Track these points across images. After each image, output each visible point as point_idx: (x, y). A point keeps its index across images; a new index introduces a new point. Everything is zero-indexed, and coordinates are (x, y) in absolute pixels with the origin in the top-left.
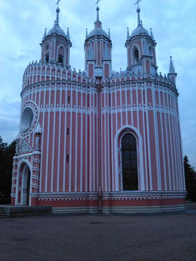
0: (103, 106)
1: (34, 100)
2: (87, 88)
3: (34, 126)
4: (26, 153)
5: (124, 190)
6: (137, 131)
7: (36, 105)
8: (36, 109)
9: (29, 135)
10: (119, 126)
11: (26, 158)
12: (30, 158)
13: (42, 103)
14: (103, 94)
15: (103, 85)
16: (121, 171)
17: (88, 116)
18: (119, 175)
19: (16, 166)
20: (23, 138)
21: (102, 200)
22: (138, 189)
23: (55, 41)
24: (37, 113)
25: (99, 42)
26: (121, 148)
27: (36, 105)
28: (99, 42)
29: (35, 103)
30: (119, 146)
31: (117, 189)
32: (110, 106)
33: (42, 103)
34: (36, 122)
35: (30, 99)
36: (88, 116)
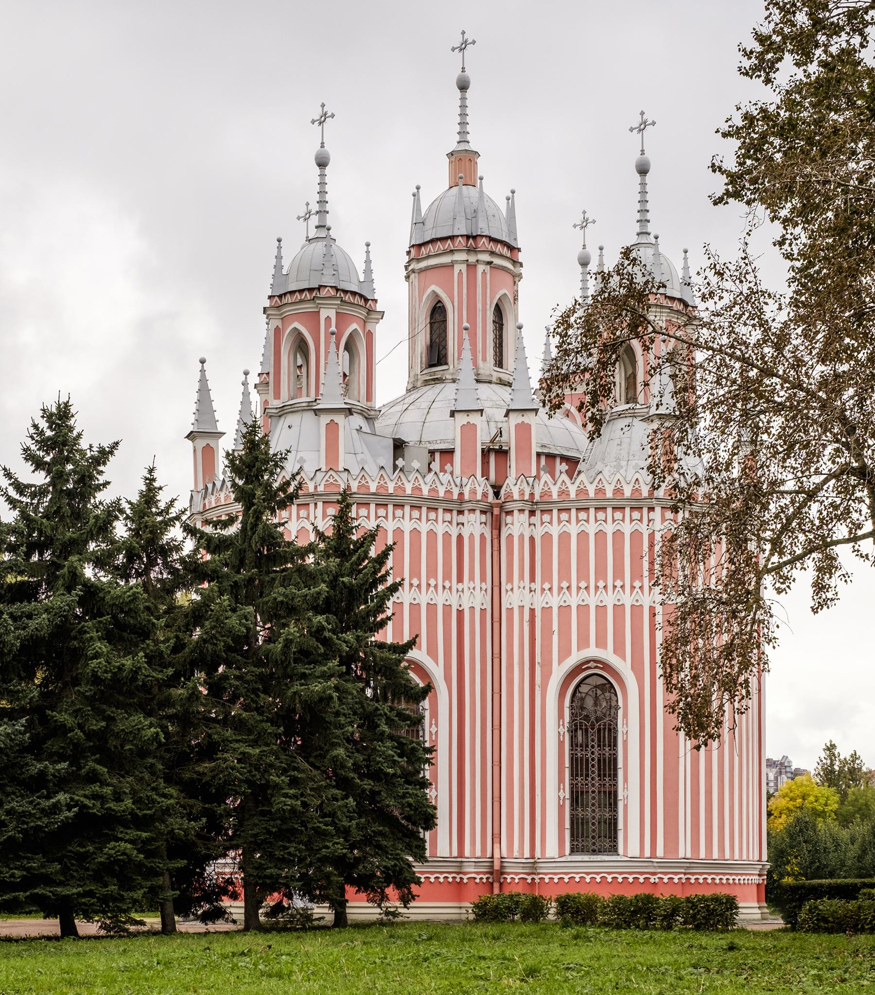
2: (455, 513)
5: (573, 851)
14: (510, 536)
15: (509, 506)
16: (568, 796)
17: (460, 613)
18: (561, 808)
21: (501, 884)
22: (614, 850)
23: (332, 314)
25: (471, 267)
26: (567, 725)
28: (471, 267)
30: (561, 716)
31: (552, 850)
32: (532, 579)
36: (460, 613)
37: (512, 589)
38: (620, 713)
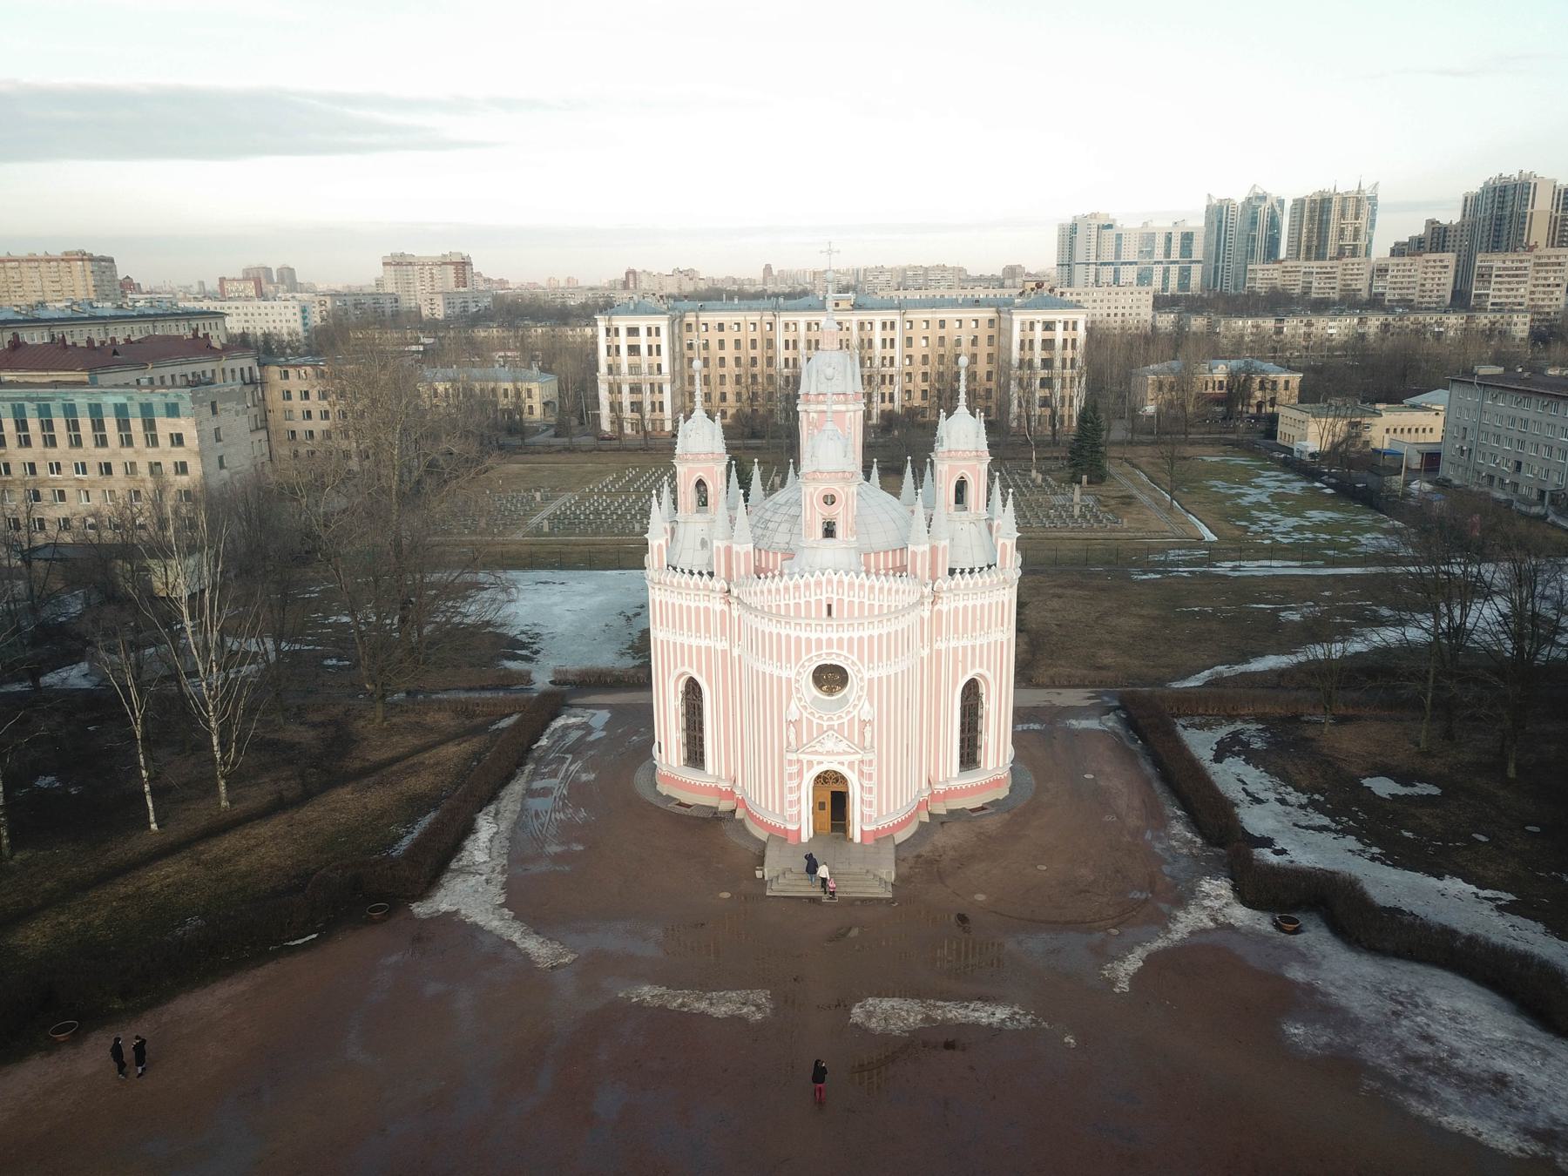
0: (939, 633)
1: (850, 650)
3: (855, 706)
4: (839, 754)
6: (990, 676)
7: (858, 663)
8: (859, 671)
9: (845, 720)
10: (965, 672)
11: (842, 764)
12: (851, 764)
13: (871, 660)
19: (800, 773)
20: (825, 724)
24: (862, 679)
27: (858, 663)
29: (855, 658)
33: (871, 660)
34: (860, 698)
35: (840, 647)
38: (984, 697)
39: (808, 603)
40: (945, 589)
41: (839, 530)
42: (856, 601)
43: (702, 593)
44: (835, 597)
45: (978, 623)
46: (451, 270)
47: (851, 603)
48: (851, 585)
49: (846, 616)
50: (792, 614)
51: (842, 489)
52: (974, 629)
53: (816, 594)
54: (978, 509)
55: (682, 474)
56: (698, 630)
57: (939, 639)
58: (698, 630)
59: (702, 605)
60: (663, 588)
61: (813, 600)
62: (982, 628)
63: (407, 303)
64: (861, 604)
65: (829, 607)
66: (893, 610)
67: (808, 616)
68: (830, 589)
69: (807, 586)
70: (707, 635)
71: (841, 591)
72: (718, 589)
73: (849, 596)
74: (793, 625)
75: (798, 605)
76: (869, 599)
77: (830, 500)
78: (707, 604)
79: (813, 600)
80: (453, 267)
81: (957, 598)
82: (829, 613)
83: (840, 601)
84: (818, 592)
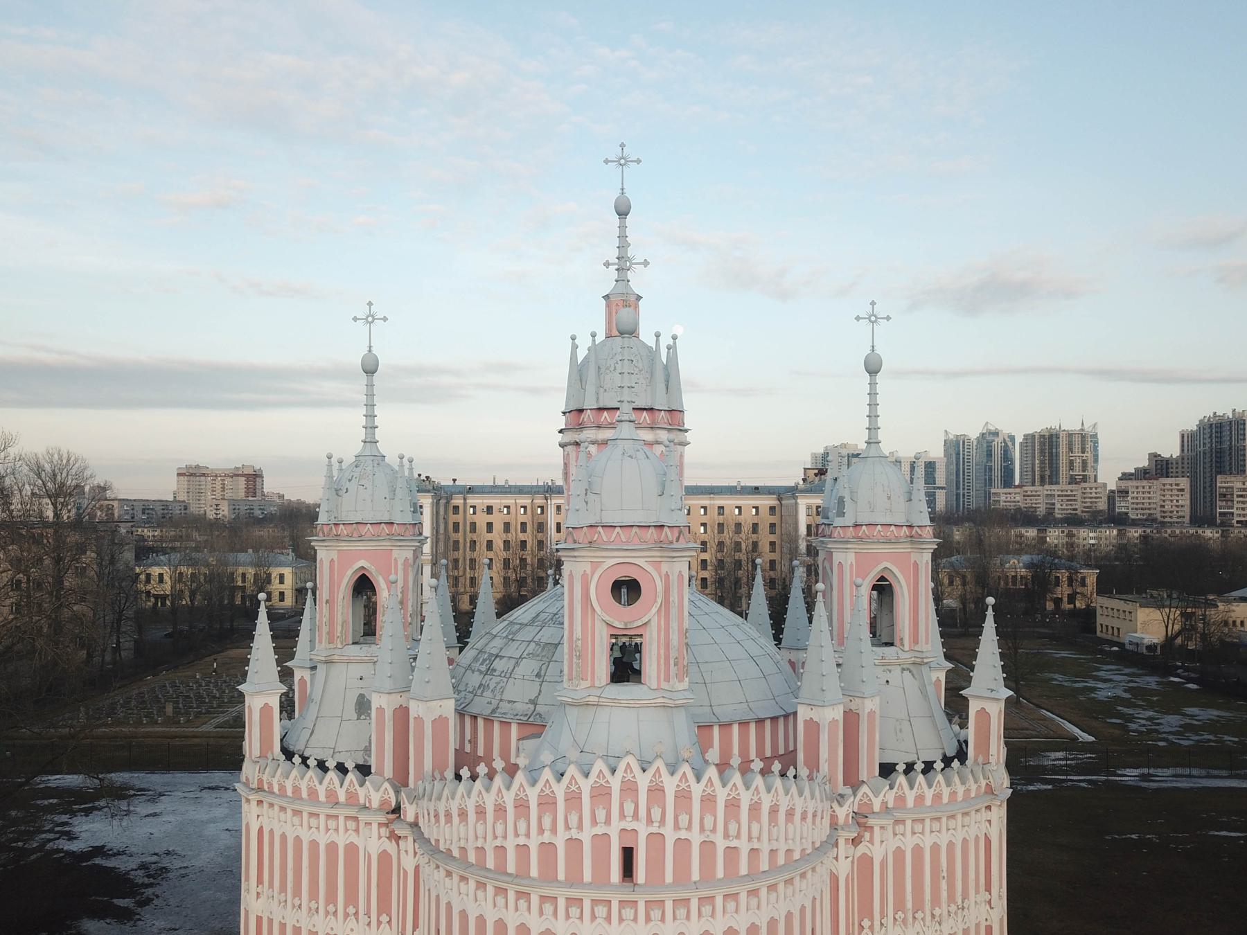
37: (871, 928)
39: (574, 845)
40: (877, 808)
41: (650, 663)
42: (696, 838)
43: (342, 812)
44: (643, 831)
45: (944, 885)
46: (242, 481)
47: (682, 845)
48: (683, 797)
49: (669, 878)
50: (534, 872)
51: (656, 565)
52: (936, 901)
53: (594, 822)
54: (916, 641)
55: (326, 565)
56: (331, 898)
57: (866, 923)
58: (331, 898)
59: (342, 840)
60: (268, 799)
61: (586, 838)
62: (951, 898)
63: (194, 509)
64: (708, 846)
65: (628, 855)
66: (781, 860)
67: (574, 879)
68: (629, 808)
69: (573, 799)
70: (351, 910)
71: (657, 814)
72: (375, 804)
73: (677, 827)
74: (535, 899)
75: (548, 849)
76: (726, 836)
77: (627, 589)
78: (353, 838)
79: (586, 838)
80: (244, 479)
81: (900, 828)
82: (628, 869)
83: (656, 840)
84: (601, 815)
